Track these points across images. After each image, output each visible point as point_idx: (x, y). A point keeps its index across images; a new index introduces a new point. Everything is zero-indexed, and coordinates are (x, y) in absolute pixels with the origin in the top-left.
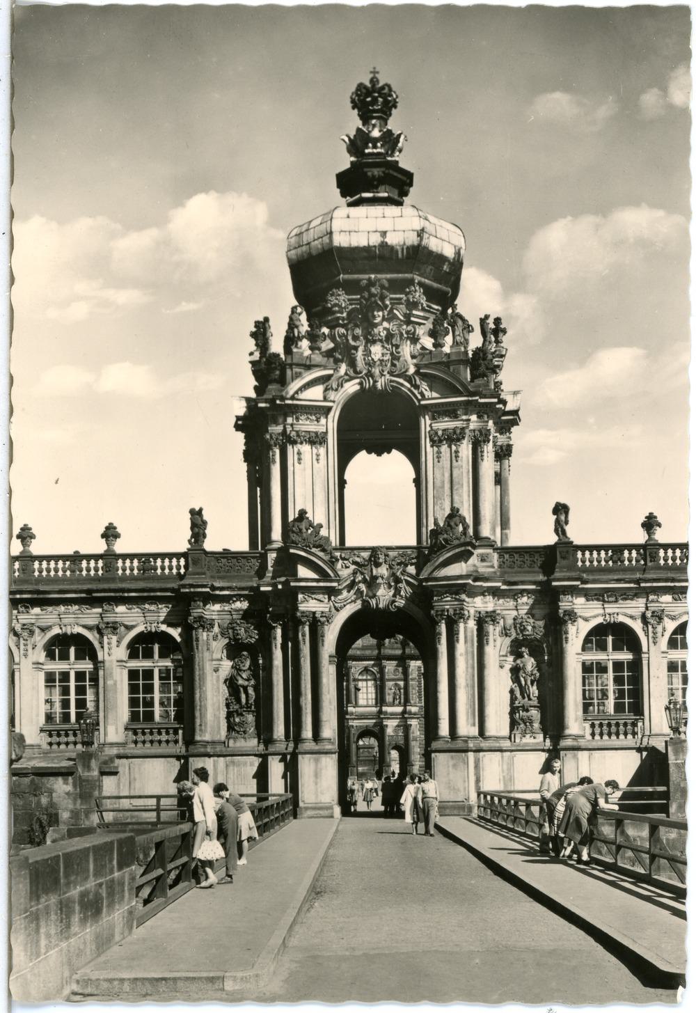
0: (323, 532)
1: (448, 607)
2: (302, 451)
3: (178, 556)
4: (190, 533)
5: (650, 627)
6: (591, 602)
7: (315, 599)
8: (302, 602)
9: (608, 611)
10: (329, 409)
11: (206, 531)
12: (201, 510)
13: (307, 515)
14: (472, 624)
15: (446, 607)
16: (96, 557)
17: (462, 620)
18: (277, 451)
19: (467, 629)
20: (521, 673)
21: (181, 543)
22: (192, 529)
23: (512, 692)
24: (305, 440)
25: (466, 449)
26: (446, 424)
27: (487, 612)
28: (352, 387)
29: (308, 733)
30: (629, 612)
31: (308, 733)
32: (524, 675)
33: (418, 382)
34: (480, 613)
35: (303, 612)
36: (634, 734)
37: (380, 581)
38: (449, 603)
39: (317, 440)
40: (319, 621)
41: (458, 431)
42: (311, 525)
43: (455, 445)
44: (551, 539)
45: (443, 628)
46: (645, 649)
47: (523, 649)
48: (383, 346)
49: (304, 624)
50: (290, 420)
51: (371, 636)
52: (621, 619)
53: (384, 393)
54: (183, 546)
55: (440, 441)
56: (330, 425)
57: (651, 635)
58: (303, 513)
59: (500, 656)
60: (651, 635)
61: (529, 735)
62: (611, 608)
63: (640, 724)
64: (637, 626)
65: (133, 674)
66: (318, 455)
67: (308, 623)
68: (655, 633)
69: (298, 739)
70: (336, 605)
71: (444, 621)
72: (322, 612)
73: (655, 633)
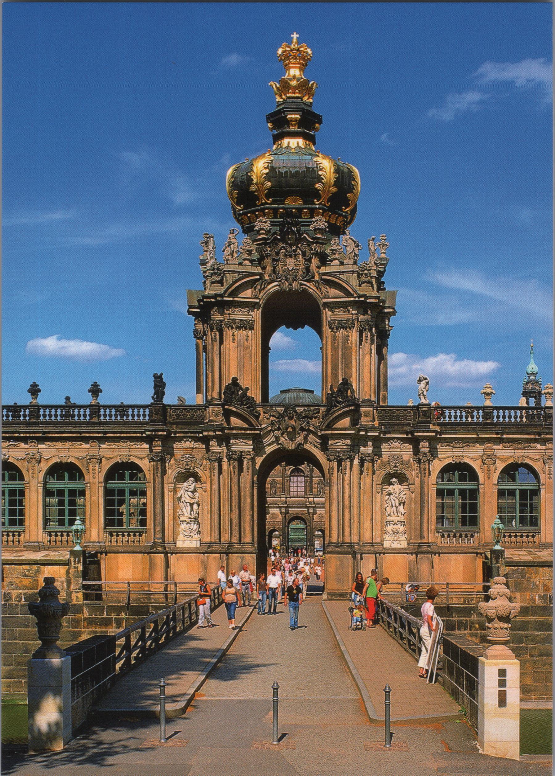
1: (339, 450)
3: (144, 407)
4: (154, 391)
11: (165, 390)
12: (162, 374)
13: (238, 382)
16: (85, 407)
21: (145, 396)
22: (155, 388)
25: (354, 335)
26: (340, 315)
28: (273, 287)
30: (471, 455)
39: (247, 326)
42: (241, 388)
43: (347, 332)
46: (481, 480)
52: (466, 460)
54: (149, 401)
56: (256, 315)
58: (235, 380)
62: (458, 452)
65: (108, 492)
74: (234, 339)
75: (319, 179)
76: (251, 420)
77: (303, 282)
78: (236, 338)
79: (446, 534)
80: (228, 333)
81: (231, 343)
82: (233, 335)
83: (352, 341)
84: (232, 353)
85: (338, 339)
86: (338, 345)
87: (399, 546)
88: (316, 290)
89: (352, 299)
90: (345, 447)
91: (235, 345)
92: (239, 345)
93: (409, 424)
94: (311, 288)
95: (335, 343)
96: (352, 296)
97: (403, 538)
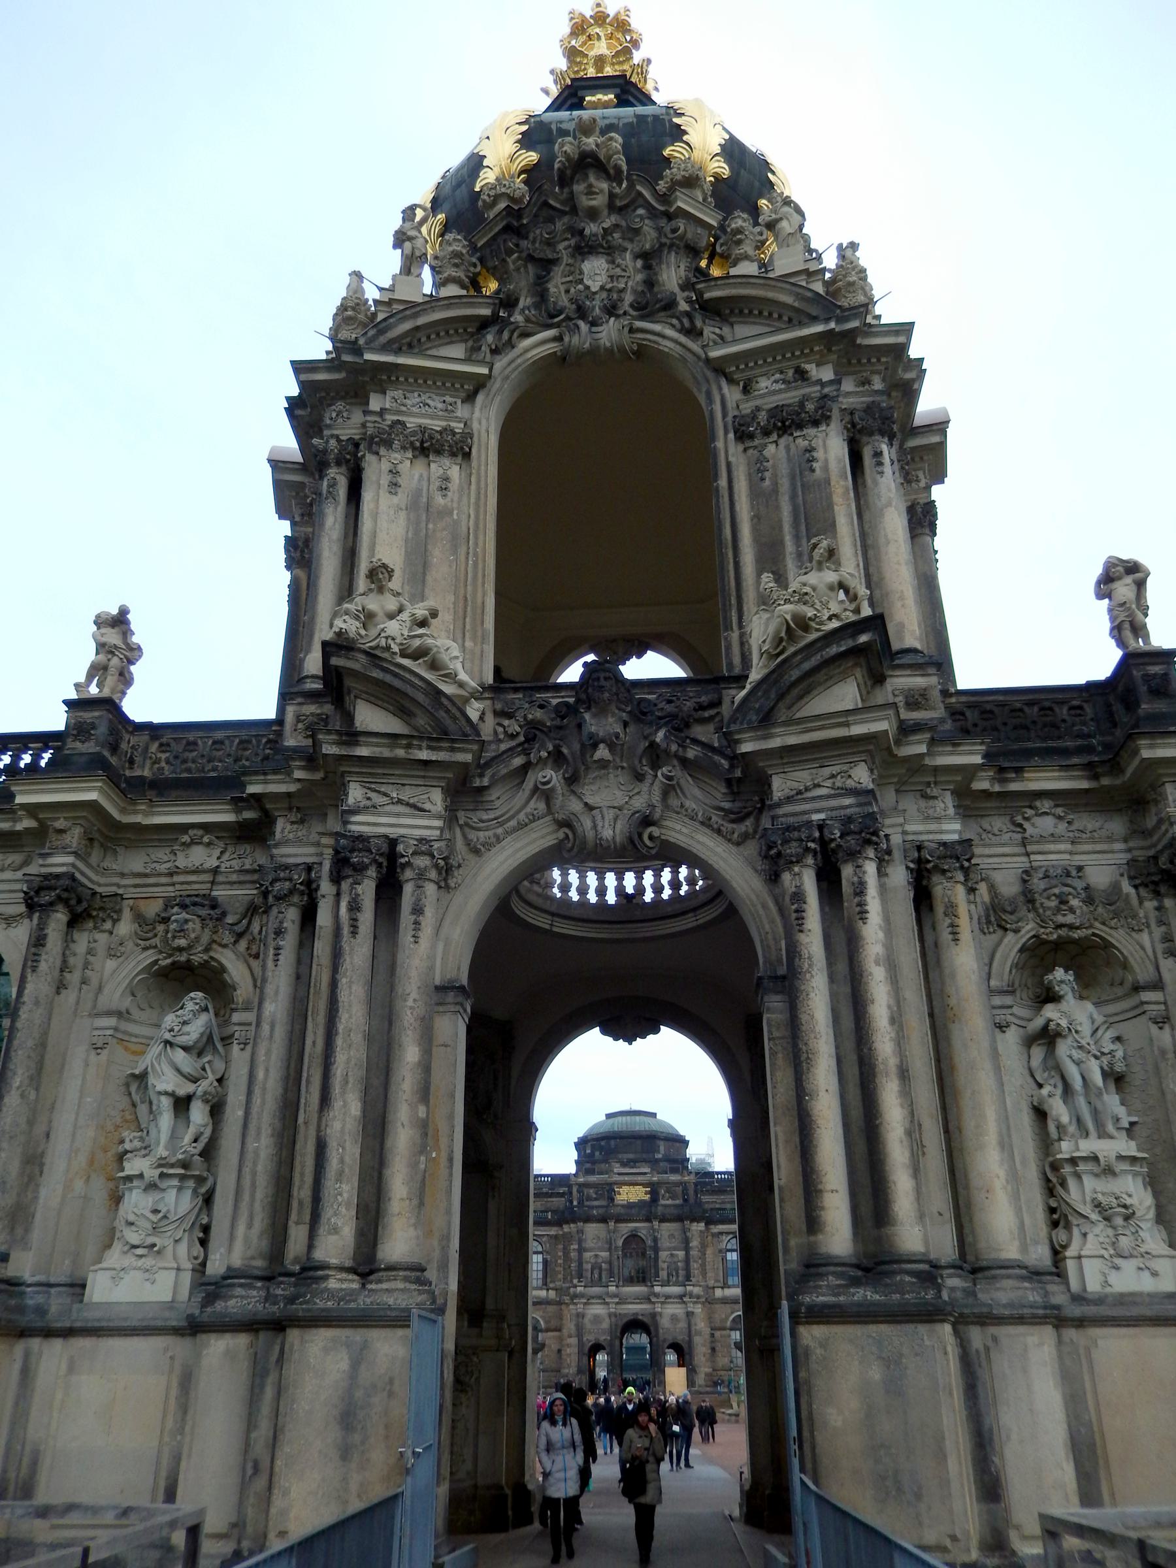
1: (822, 816)
7: (400, 802)
14: (899, 875)
17: (871, 853)
19: (881, 898)
23: (1040, 1114)
25: (832, 447)
28: (536, 346)
29: (336, 1243)
32: (1076, 1054)
33: (699, 323)
34: (919, 848)
35: (361, 838)
40: (408, 864)
47: (1059, 973)
50: (375, 403)
51: (605, 1032)
59: (992, 992)
71: (810, 860)
72: (422, 840)
74: (394, 485)
80: (375, 470)
82: (394, 472)
83: (826, 460)
84: (383, 523)
86: (775, 484)
87: (1146, 1284)
88: (683, 339)
90: (847, 801)
91: (401, 499)
92: (413, 506)
93: (1090, 750)
94: (665, 335)
95: (763, 479)
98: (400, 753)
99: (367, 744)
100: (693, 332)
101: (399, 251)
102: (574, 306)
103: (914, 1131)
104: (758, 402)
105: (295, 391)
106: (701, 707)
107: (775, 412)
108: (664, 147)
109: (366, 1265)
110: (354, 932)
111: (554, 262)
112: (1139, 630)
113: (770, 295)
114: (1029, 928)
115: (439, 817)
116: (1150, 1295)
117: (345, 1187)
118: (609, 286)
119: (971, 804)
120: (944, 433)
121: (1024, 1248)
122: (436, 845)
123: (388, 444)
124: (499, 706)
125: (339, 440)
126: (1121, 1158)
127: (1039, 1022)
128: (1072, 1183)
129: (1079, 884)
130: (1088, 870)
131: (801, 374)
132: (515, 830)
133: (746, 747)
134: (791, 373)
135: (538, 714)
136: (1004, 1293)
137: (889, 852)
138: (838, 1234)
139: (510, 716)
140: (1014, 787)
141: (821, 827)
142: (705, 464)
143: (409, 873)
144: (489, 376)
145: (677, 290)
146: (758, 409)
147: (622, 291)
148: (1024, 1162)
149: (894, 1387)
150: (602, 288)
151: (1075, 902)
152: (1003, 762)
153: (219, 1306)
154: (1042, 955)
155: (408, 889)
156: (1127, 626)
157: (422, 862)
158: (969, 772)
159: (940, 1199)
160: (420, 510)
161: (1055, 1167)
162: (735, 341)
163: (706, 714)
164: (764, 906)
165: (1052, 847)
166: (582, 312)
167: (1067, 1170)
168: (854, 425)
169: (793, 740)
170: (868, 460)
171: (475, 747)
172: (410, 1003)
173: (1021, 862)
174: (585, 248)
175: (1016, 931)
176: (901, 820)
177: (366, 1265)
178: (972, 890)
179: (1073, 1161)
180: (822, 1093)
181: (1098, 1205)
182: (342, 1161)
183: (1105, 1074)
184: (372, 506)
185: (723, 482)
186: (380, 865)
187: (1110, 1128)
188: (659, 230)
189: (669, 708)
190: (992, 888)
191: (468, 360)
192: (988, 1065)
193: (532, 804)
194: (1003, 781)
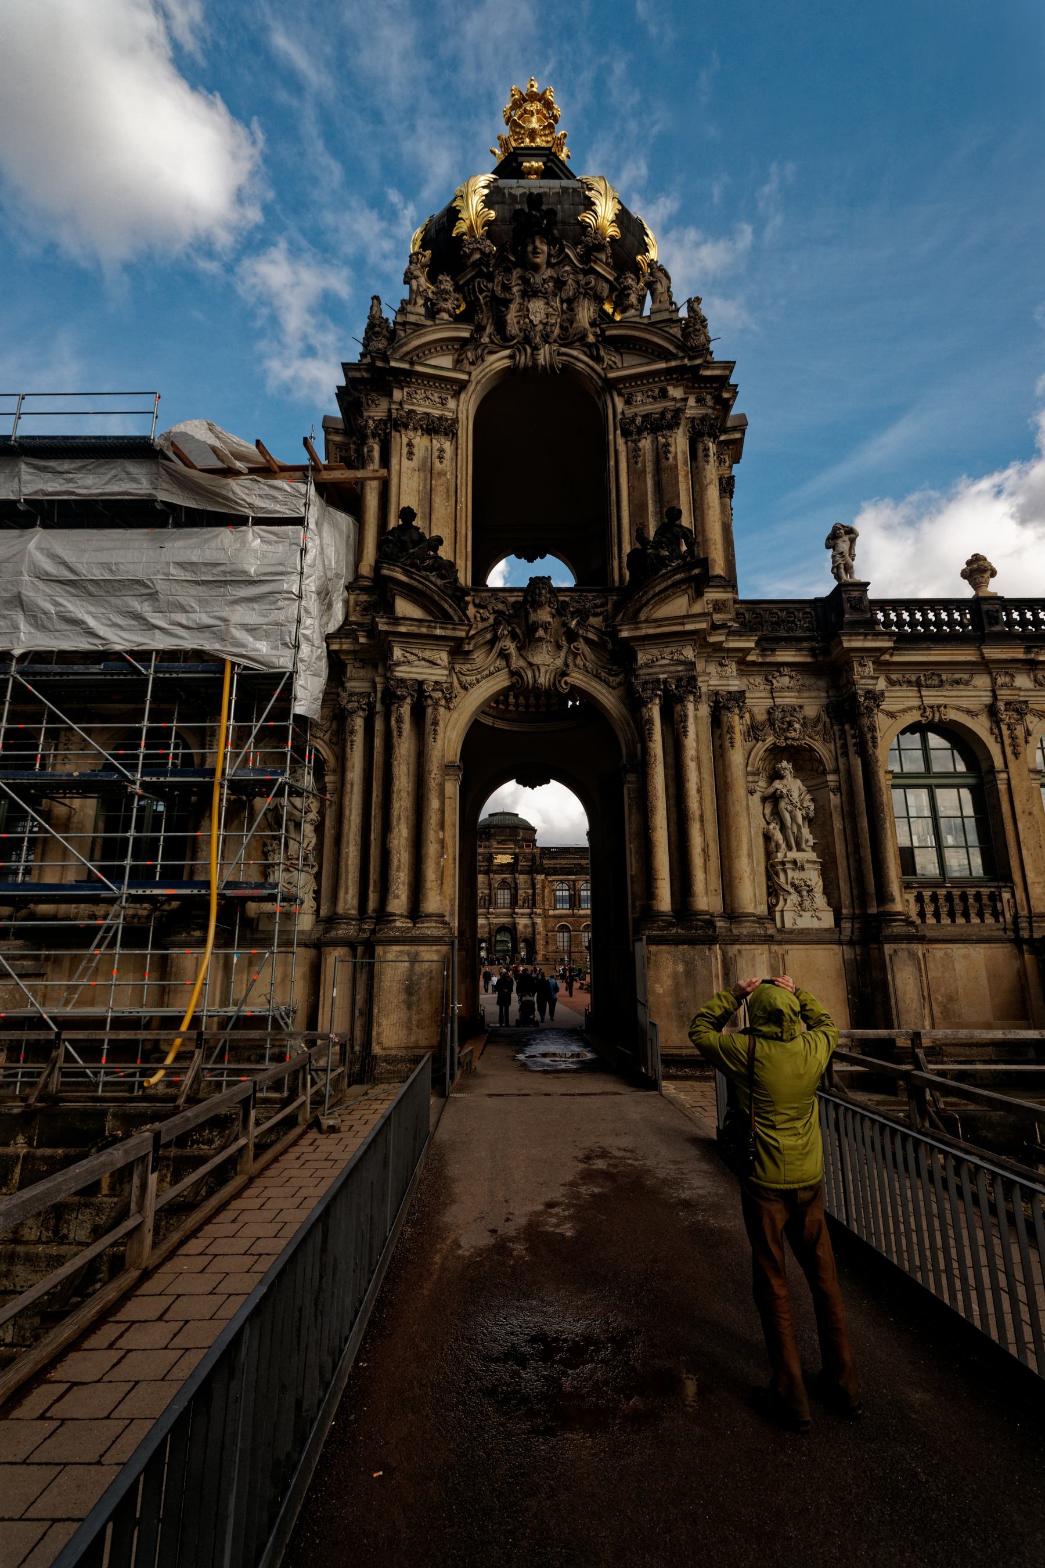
0: (444, 552)
1: (665, 676)
2: (415, 442)
5: (1004, 727)
6: (897, 688)
7: (424, 659)
8: (399, 664)
9: (927, 701)
10: (463, 385)
14: (704, 710)
15: (661, 676)
17: (692, 698)
18: (376, 448)
20: (783, 804)
23: (767, 838)
24: (421, 426)
25: (680, 442)
27: (730, 693)
28: (498, 361)
29: (399, 902)
30: (965, 703)
31: (399, 902)
32: (789, 808)
33: (602, 353)
34: (717, 694)
35: (402, 681)
36: (996, 914)
37: (541, 633)
38: (667, 669)
40: (430, 697)
41: (669, 416)
43: (663, 436)
44: (823, 587)
45: (655, 712)
46: (998, 763)
47: (784, 764)
48: (547, 304)
49: (402, 698)
53: (548, 373)
55: (640, 431)
57: (1007, 741)
60: (1007, 741)
61: (810, 913)
62: (932, 697)
63: (1006, 896)
64: (980, 726)
66: (442, 451)
67: (409, 700)
68: (1013, 738)
69: (383, 916)
70: (463, 678)
71: (657, 701)
72: (436, 682)
73: (1013, 738)
74: (410, 454)
75: (589, 205)
76: (446, 606)
77: (563, 350)
78: (415, 450)
79: (927, 894)
81: (405, 460)
84: (404, 480)
85: (644, 454)
86: (644, 466)
87: (815, 924)
88: (591, 363)
89: (673, 364)
90: (680, 668)
95: (636, 463)
96: (675, 357)
97: (820, 900)
98: (424, 630)
99: (404, 625)
100: (599, 359)
101: (408, 286)
102: (522, 334)
103: (705, 851)
104: (636, 410)
105: (343, 383)
106: (596, 606)
107: (646, 417)
108: (579, 215)
109: (415, 912)
110: (400, 735)
111: (511, 301)
112: (848, 569)
113: (648, 336)
114: (770, 740)
115: (445, 668)
116: (817, 929)
117: (402, 875)
118: (545, 321)
119: (745, 667)
120: (743, 432)
121: (755, 907)
122: (445, 685)
123: (406, 426)
124: (477, 601)
125: (374, 421)
126: (808, 861)
127: (771, 790)
128: (782, 876)
129: (801, 716)
130: (805, 707)
131: (664, 394)
132: (487, 676)
133: (624, 634)
134: (657, 391)
135: (500, 607)
136: (745, 929)
137: (700, 697)
138: (664, 901)
139: (484, 607)
140: (769, 659)
141: (665, 681)
142: (601, 449)
143: (430, 702)
144: (469, 381)
145: (587, 326)
146: (636, 415)
147: (552, 325)
148: (758, 864)
149: (690, 973)
150: (541, 322)
151: (797, 726)
152: (767, 644)
153: (333, 934)
154: (775, 753)
155: (430, 710)
156: (842, 566)
157: (437, 695)
158: (747, 651)
159: (715, 883)
160: (428, 470)
161: (773, 866)
162: (623, 368)
163: (599, 610)
164: (628, 724)
165: (787, 694)
166: (527, 340)
167: (779, 867)
168: (693, 428)
169: (651, 631)
170: (700, 454)
171: (467, 628)
172: (433, 776)
173: (769, 703)
174: (530, 293)
175: (763, 741)
176: (707, 678)
177: (415, 912)
178: (742, 717)
179: (783, 863)
180: (659, 829)
181: (793, 885)
182: (399, 861)
183: (804, 818)
184: (397, 467)
185: (612, 463)
186: (412, 696)
187: (804, 846)
188: (577, 282)
189: (578, 606)
190: (752, 716)
191: (454, 369)
192: (745, 814)
193: (498, 662)
194: (763, 656)
